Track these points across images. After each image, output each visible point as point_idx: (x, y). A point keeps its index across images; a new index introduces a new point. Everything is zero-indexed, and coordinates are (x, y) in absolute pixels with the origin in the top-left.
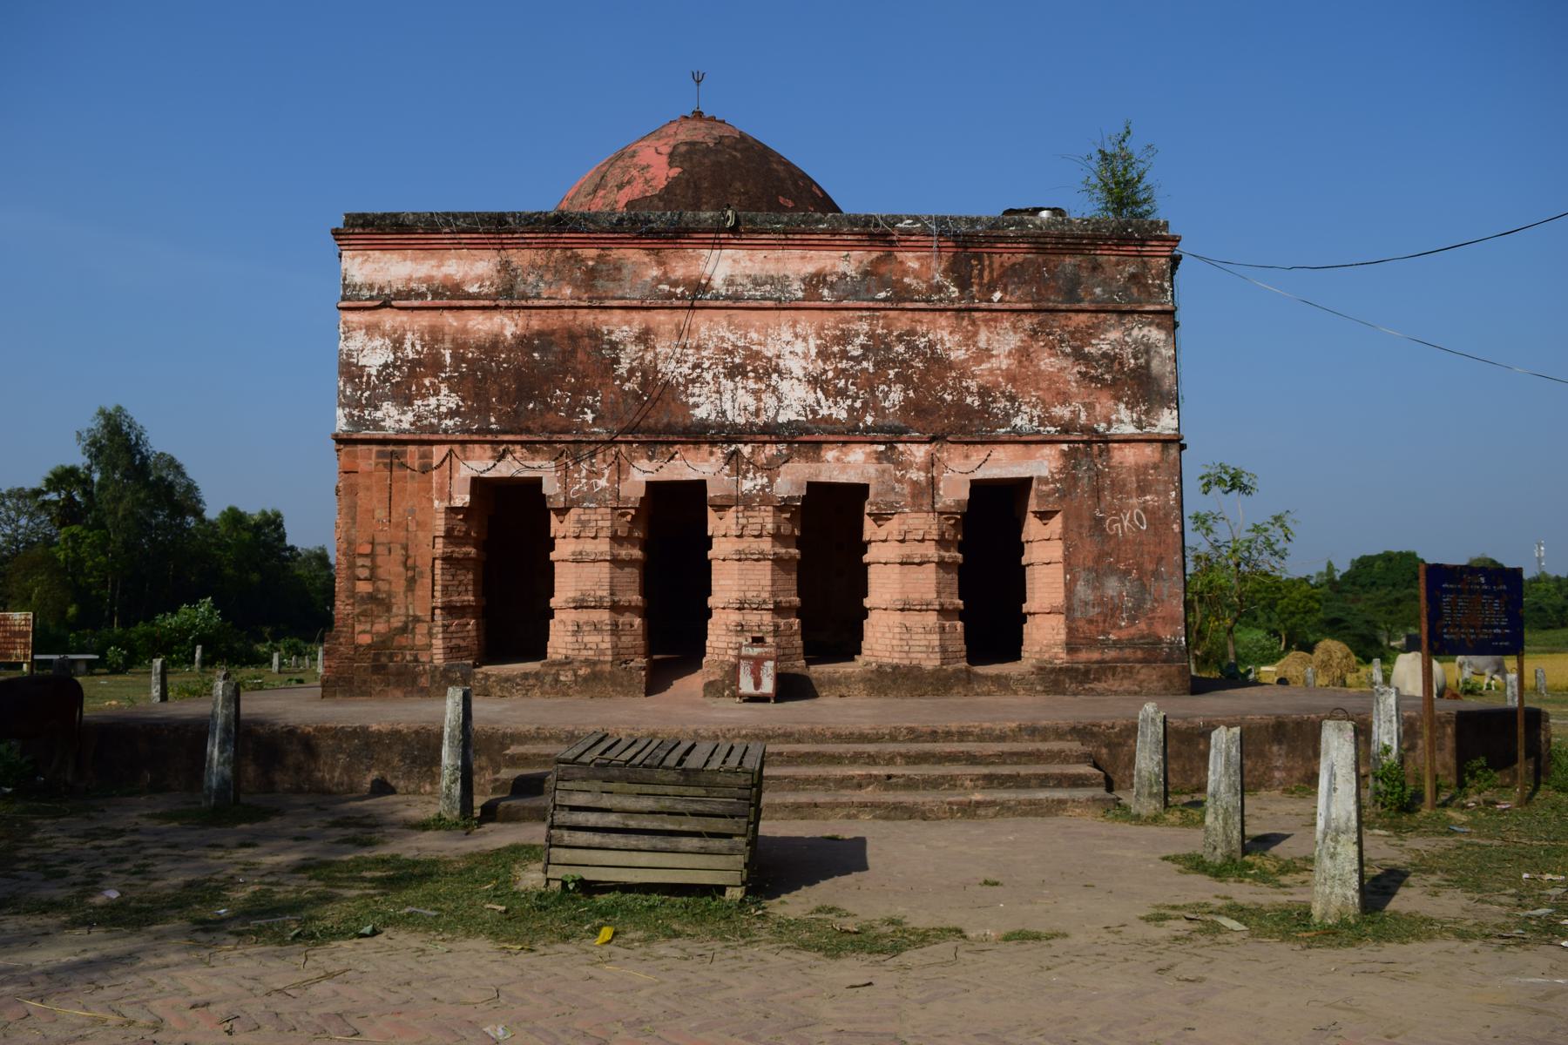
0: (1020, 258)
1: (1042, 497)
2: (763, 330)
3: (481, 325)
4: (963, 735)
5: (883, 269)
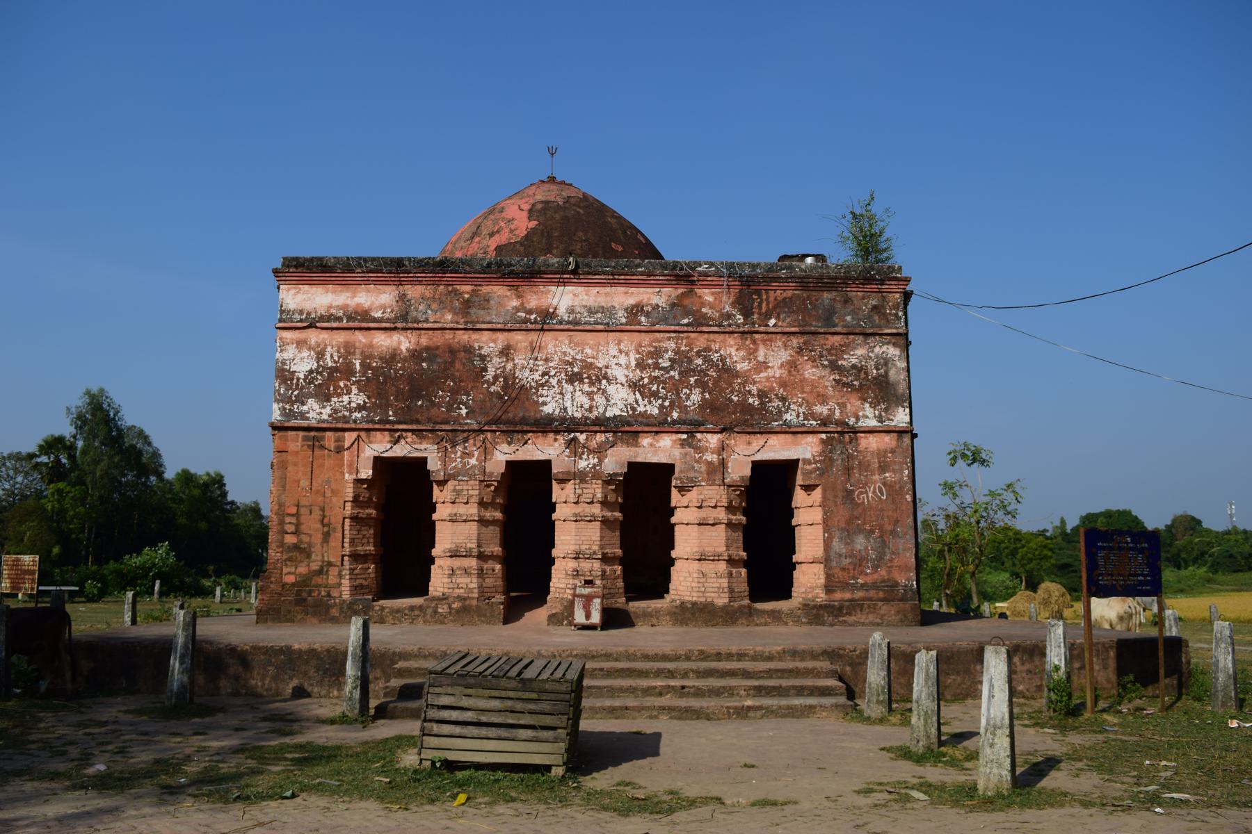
0: (789, 293)
1: (803, 474)
2: (596, 347)
3: (383, 341)
4: (741, 656)
5: (686, 302)
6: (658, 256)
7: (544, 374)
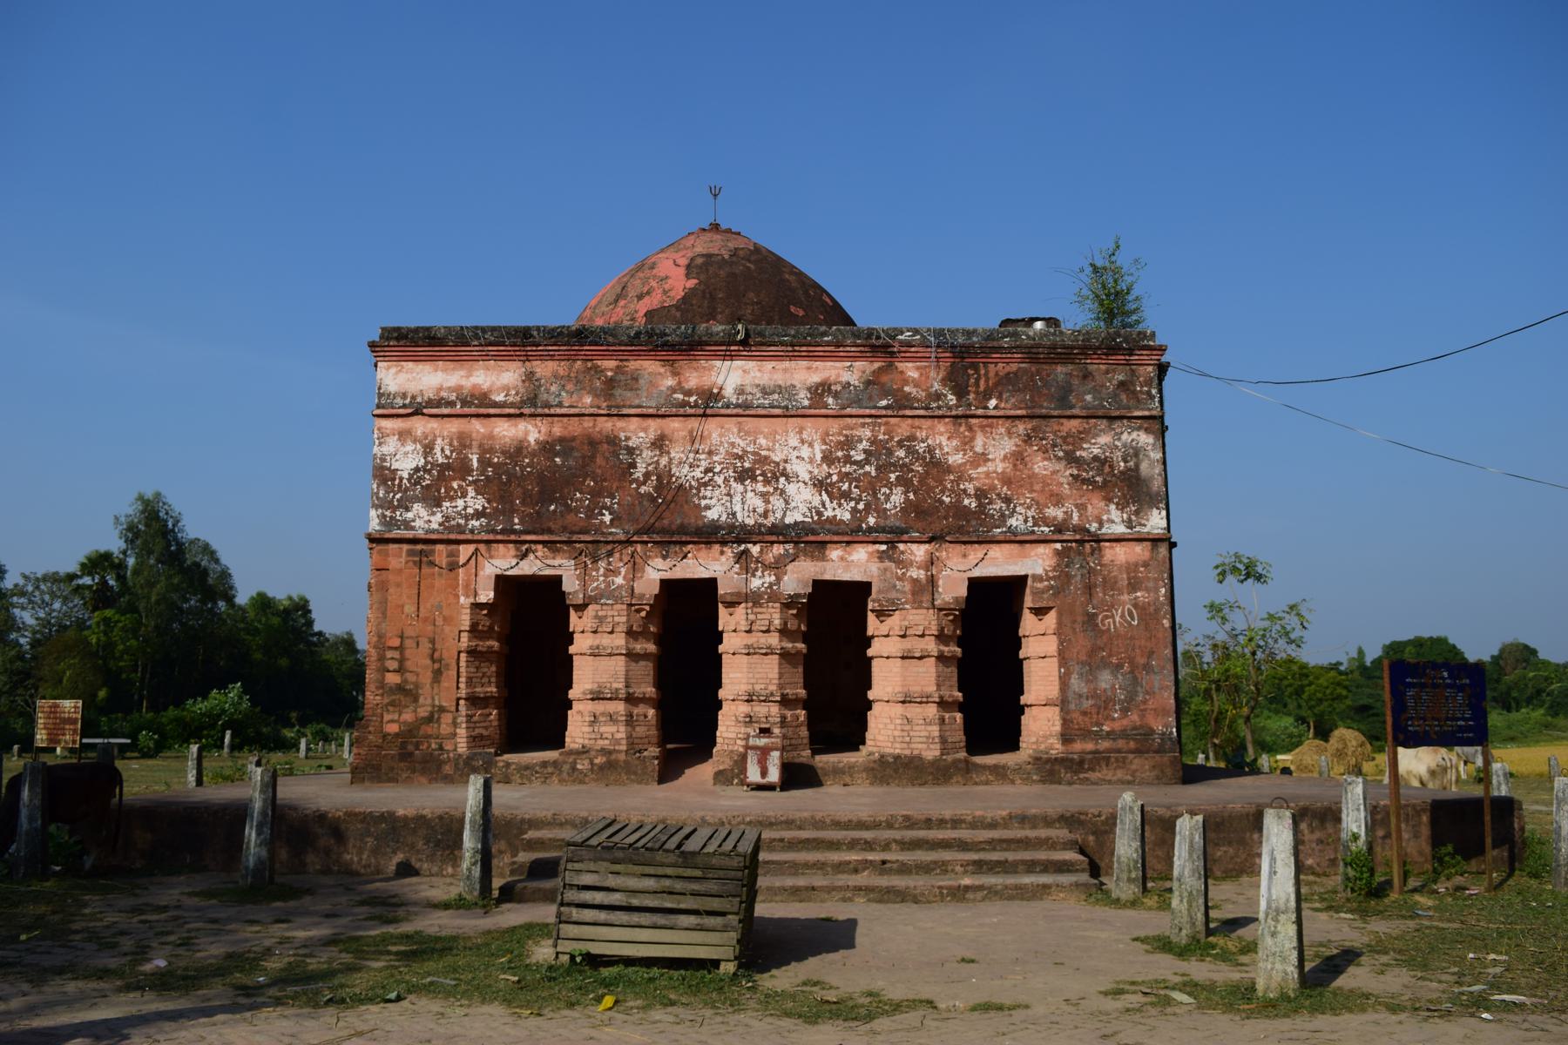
0: (1014, 367)
1: (1036, 593)
2: (772, 436)
3: (507, 431)
4: (956, 823)
5: (885, 379)
6: (849, 321)
7: (707, 471)
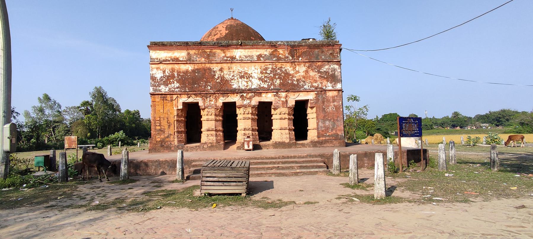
1: (311, 103)
2: (248, 68)
4: (295, 157)
7: (233, 76)
